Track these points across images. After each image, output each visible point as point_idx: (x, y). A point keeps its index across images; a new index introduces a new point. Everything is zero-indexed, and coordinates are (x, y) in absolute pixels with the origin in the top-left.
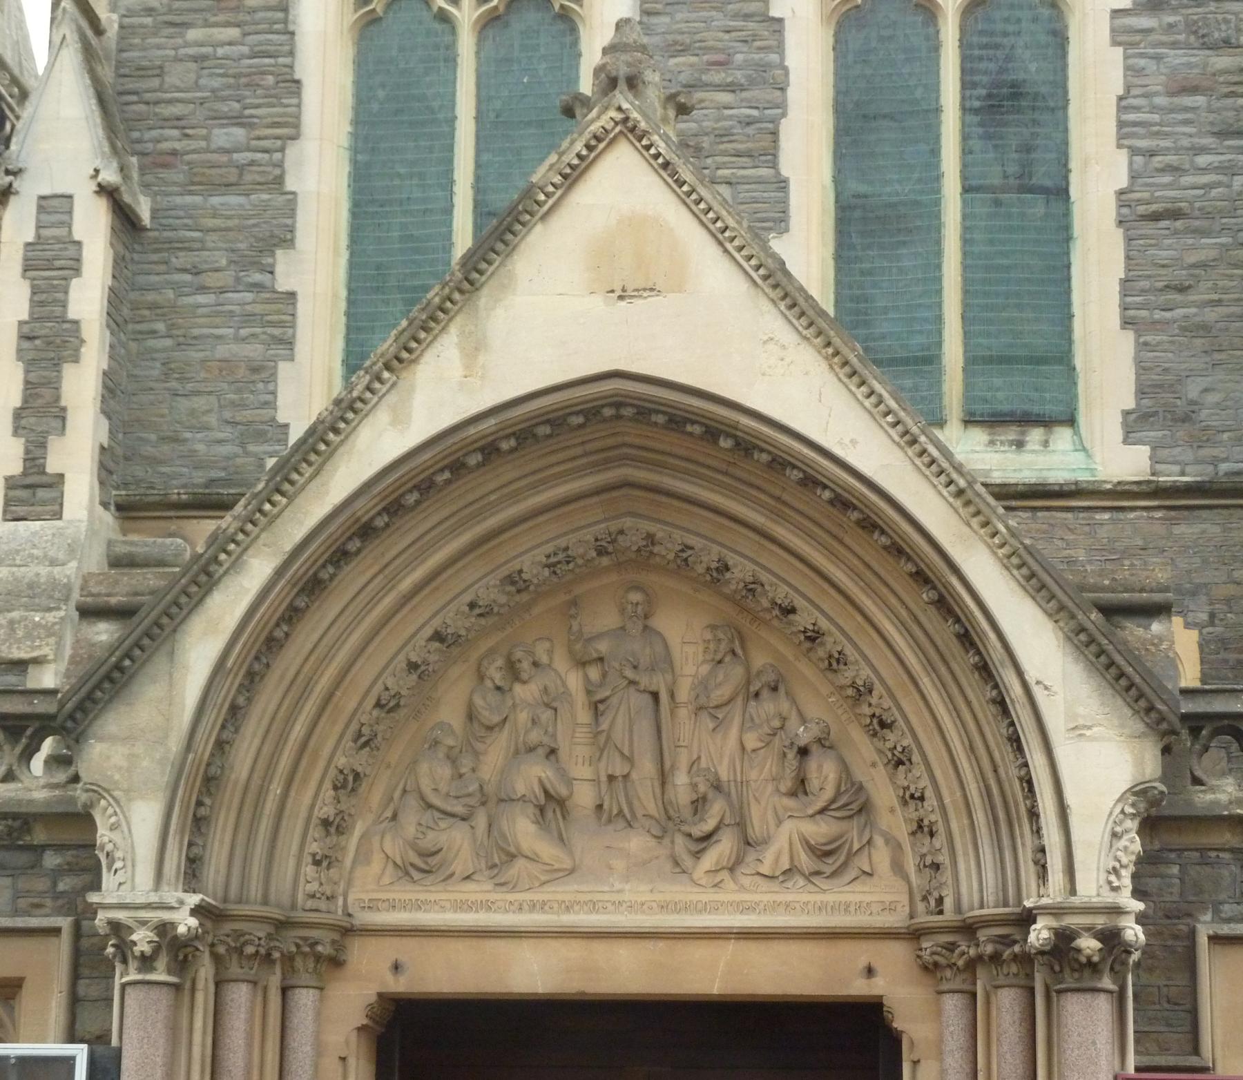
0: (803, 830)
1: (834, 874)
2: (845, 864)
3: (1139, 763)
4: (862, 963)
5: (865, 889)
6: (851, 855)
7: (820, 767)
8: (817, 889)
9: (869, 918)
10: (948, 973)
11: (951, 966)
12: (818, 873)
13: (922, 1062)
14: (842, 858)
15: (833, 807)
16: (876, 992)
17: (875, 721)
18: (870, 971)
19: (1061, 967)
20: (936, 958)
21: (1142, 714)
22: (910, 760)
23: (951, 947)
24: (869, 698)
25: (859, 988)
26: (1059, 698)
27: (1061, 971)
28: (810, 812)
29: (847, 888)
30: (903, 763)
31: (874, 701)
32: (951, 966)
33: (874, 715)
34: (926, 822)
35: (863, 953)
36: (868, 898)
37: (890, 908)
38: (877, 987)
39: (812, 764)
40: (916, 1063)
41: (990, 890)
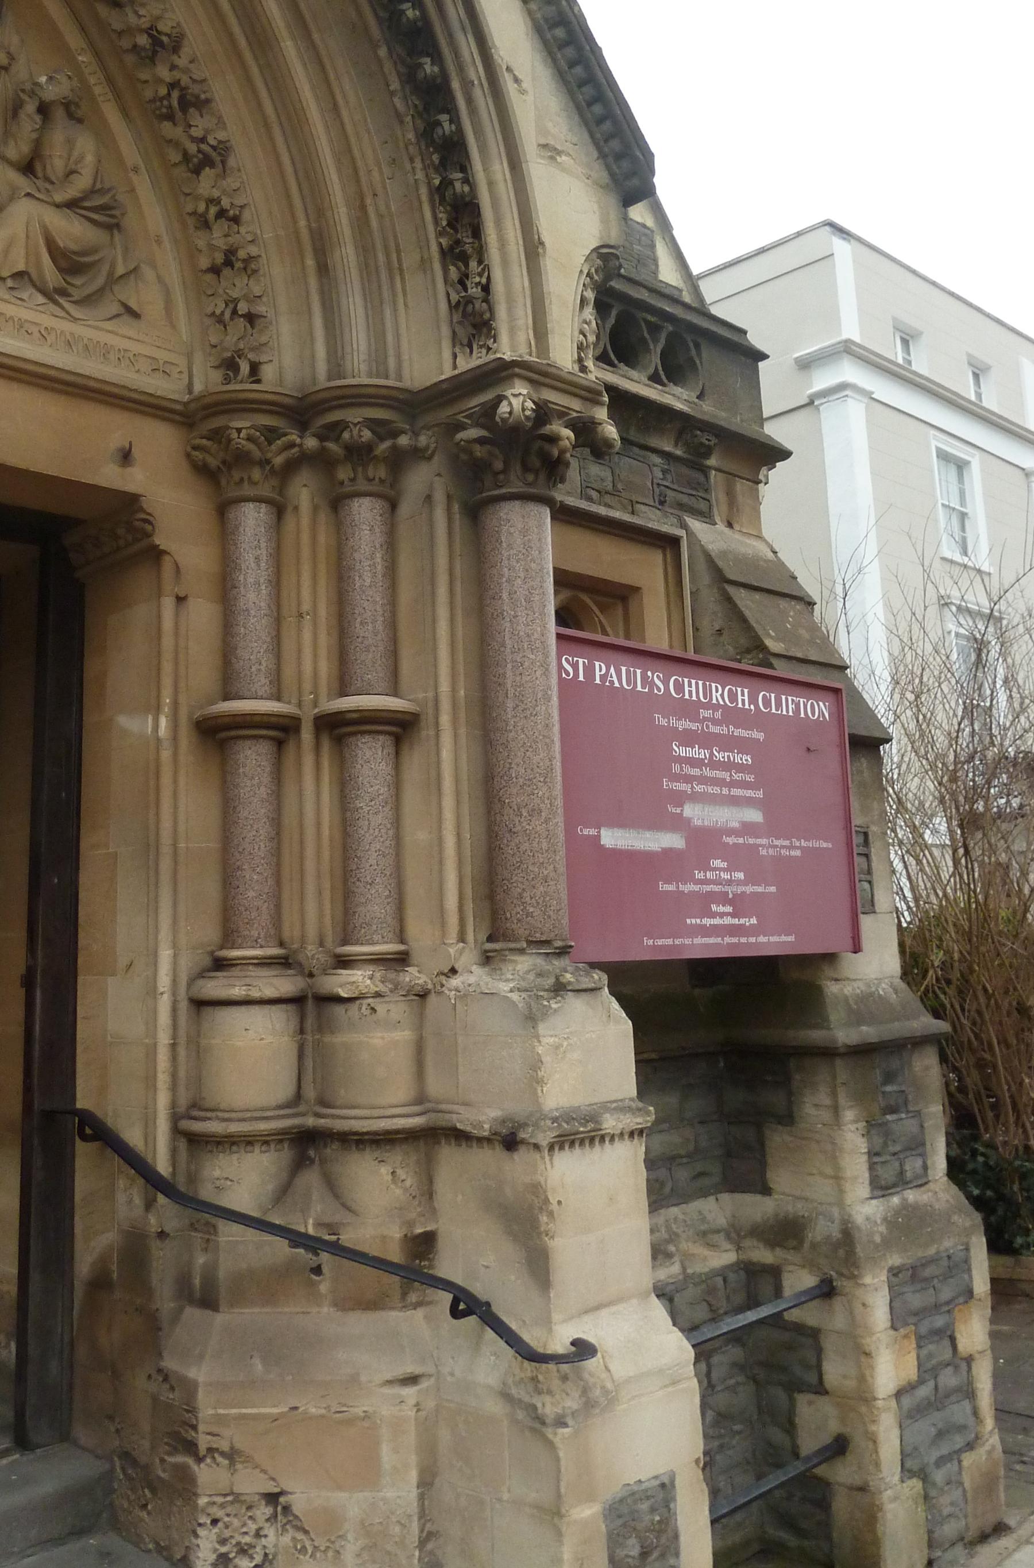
0: (47, 220)
1: (86, 301)
2: (101, 291)
3: (605, 221)
4: (117, 440)
5: (131, 333)
6: (113, 280)
7: (70, 142)
8: (63, 314)
9: (135, 376)
10: (256, 474)
11: (264, 463)
12: (63, 293)
13: (191, 601)
14: (100, 281)
15: (87, 204)
16: (131, 488)
17: (175, 94)
18: (126, 457)
19: (506, 463)
20: (251, 447)
21: (610, 159)
22: (223, 162)
23: (271, 434)
24: (175, 57)
25: (109, 476)
26: (530, 98)
27: (504, 471)
28: (58, 198)
29: (108, 325)
30: (212, 164)
31: (182, 61)
32: (264, 463)
33: (173, 86)
34: (242, 254)
35: (119, 428)
36: (135, 348)
37: (160, 369)
38: (133, 480)
39: (58, 135)
40: (180, 600)
41: (362, 357)
